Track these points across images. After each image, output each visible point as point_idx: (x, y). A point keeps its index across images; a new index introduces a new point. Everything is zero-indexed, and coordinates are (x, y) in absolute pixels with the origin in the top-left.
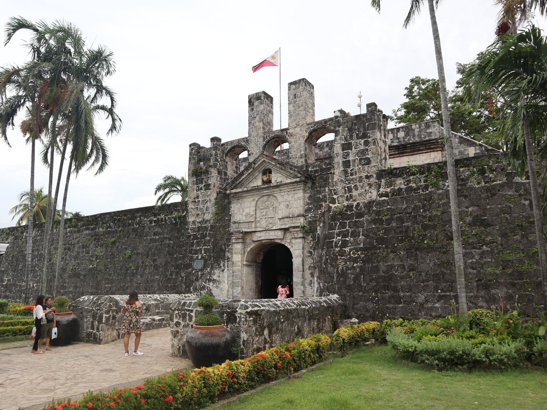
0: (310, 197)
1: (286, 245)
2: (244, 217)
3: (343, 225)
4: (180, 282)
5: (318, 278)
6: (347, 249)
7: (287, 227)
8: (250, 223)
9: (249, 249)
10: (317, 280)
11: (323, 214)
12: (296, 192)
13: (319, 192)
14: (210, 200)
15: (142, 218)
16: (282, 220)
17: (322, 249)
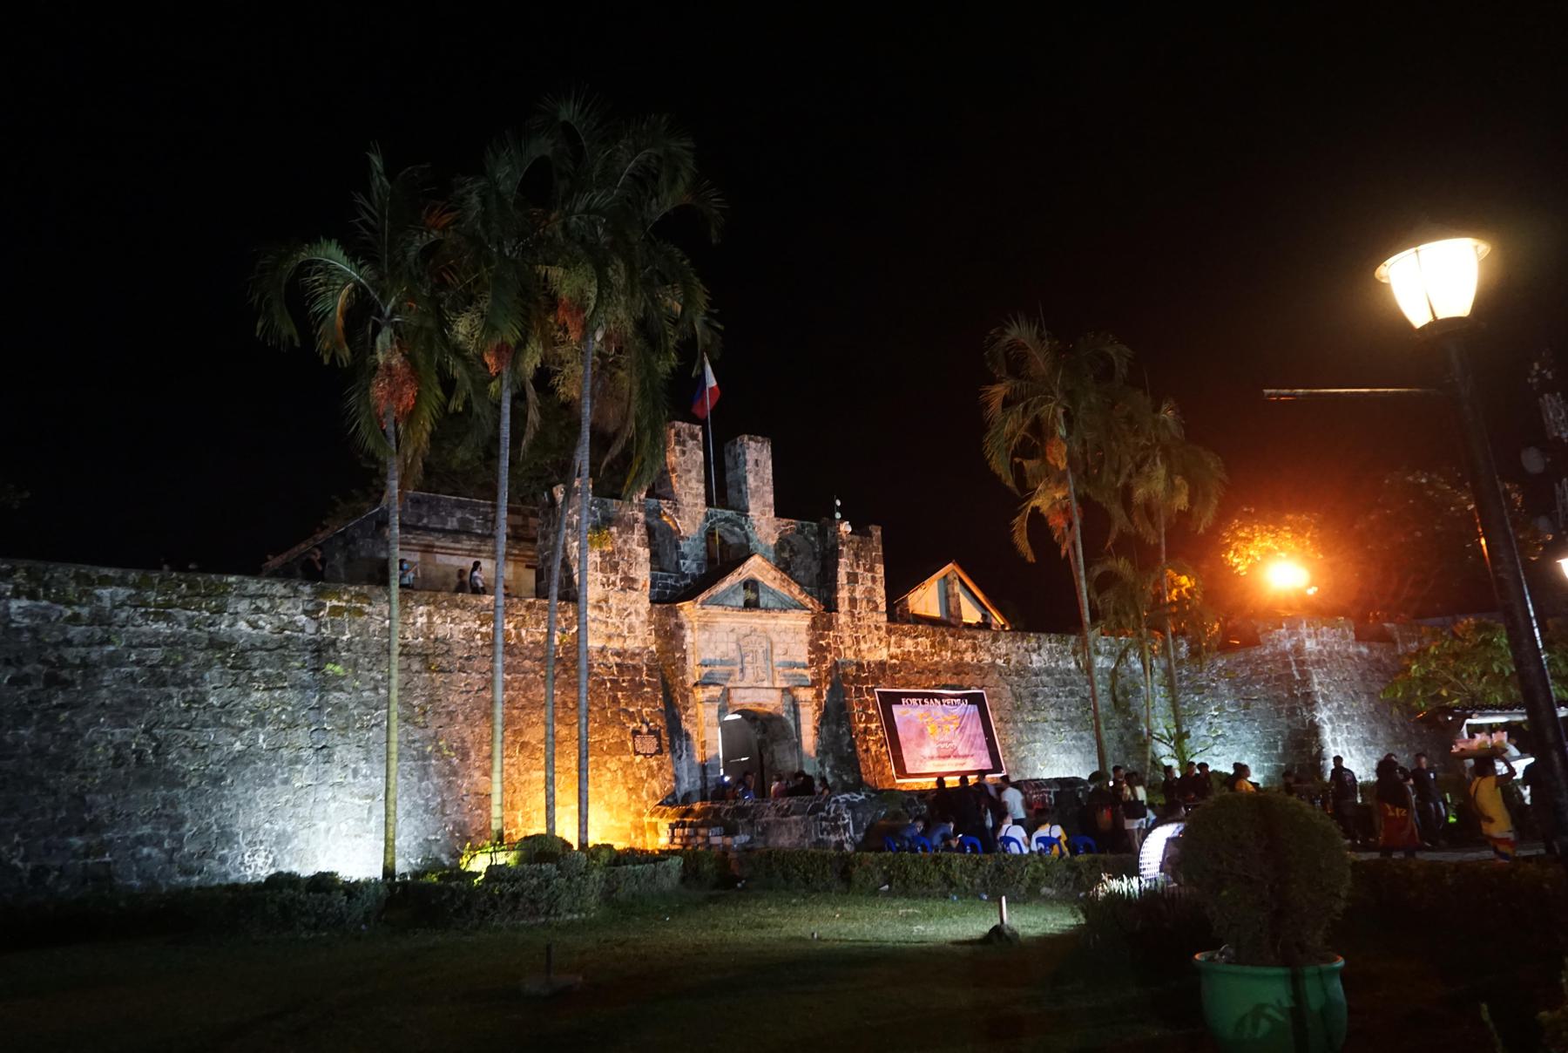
0: (811, 643)
3: (859, 690)
5: (832, 768)
6: (873, 726)
10: (831, 772)
11: (829, 672)
13: (822, 637)
14: (637, 613)
15: (437, 619)
17: (839, 725)
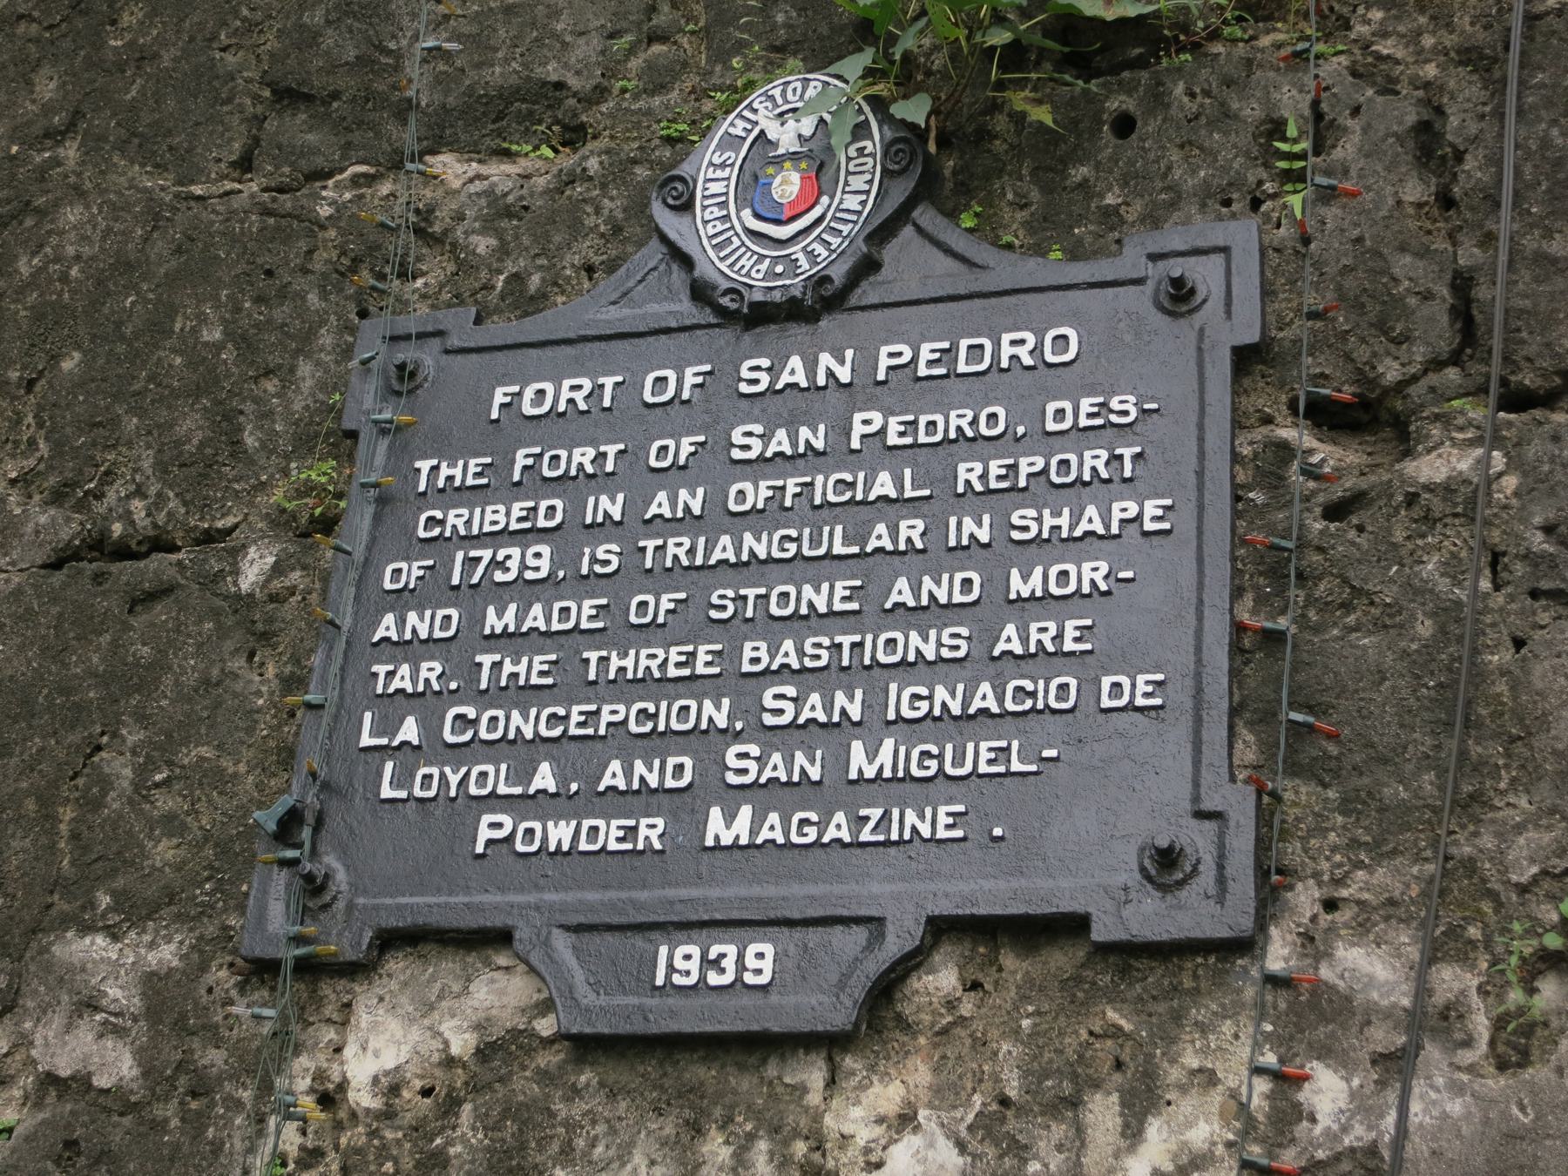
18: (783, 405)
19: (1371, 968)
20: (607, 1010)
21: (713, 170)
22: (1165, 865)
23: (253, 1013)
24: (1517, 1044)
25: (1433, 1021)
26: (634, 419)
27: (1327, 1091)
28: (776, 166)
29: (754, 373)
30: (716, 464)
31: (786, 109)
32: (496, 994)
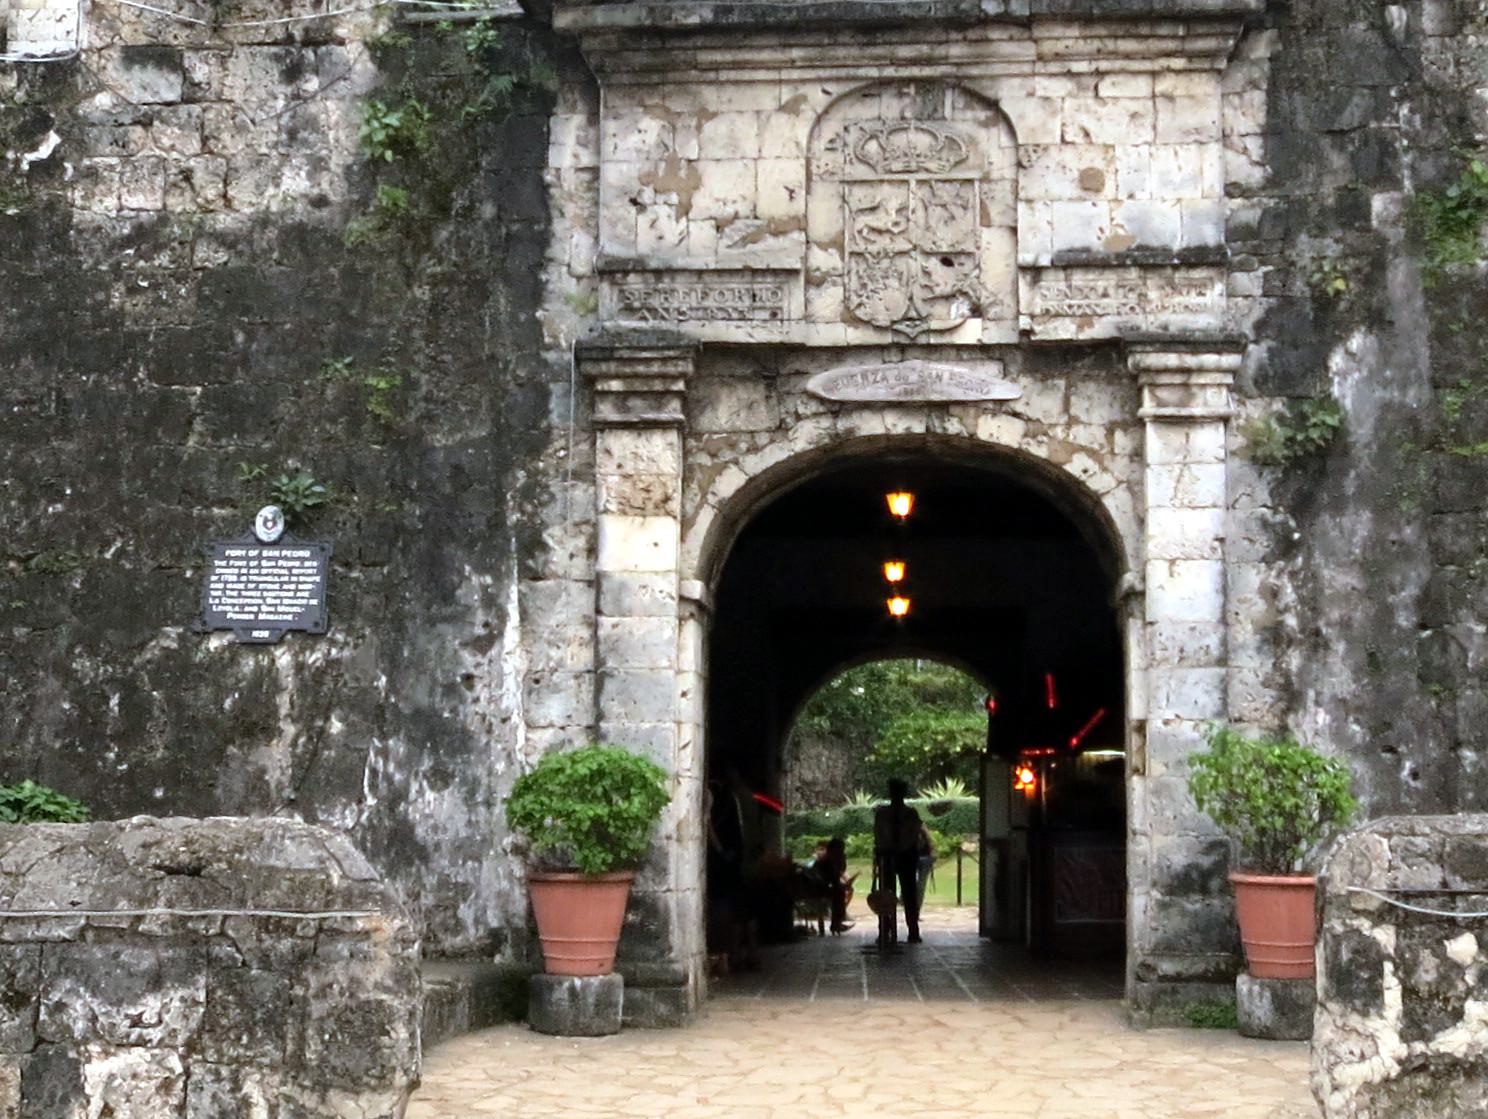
1: (1076, 466)
2: (702, 233)
4: (67, 728)
7: (1100, 330)
8: (764, 287)
9: (730, 483)
12: (1165, 85)
16: (1054, 282)
18: (269, 559)
19: (340, 637)
20: (245, 639)
21: (259, 521)
22: (316, 624)
23: (196, 639)
24: (356, 646)
25: (346, 644)
26: (248, 558)
27: (334, 651)
28: (267, 523)
29: (265, 553)
30: (259, 567)
31: (268, 511)
32: (230, 637)
